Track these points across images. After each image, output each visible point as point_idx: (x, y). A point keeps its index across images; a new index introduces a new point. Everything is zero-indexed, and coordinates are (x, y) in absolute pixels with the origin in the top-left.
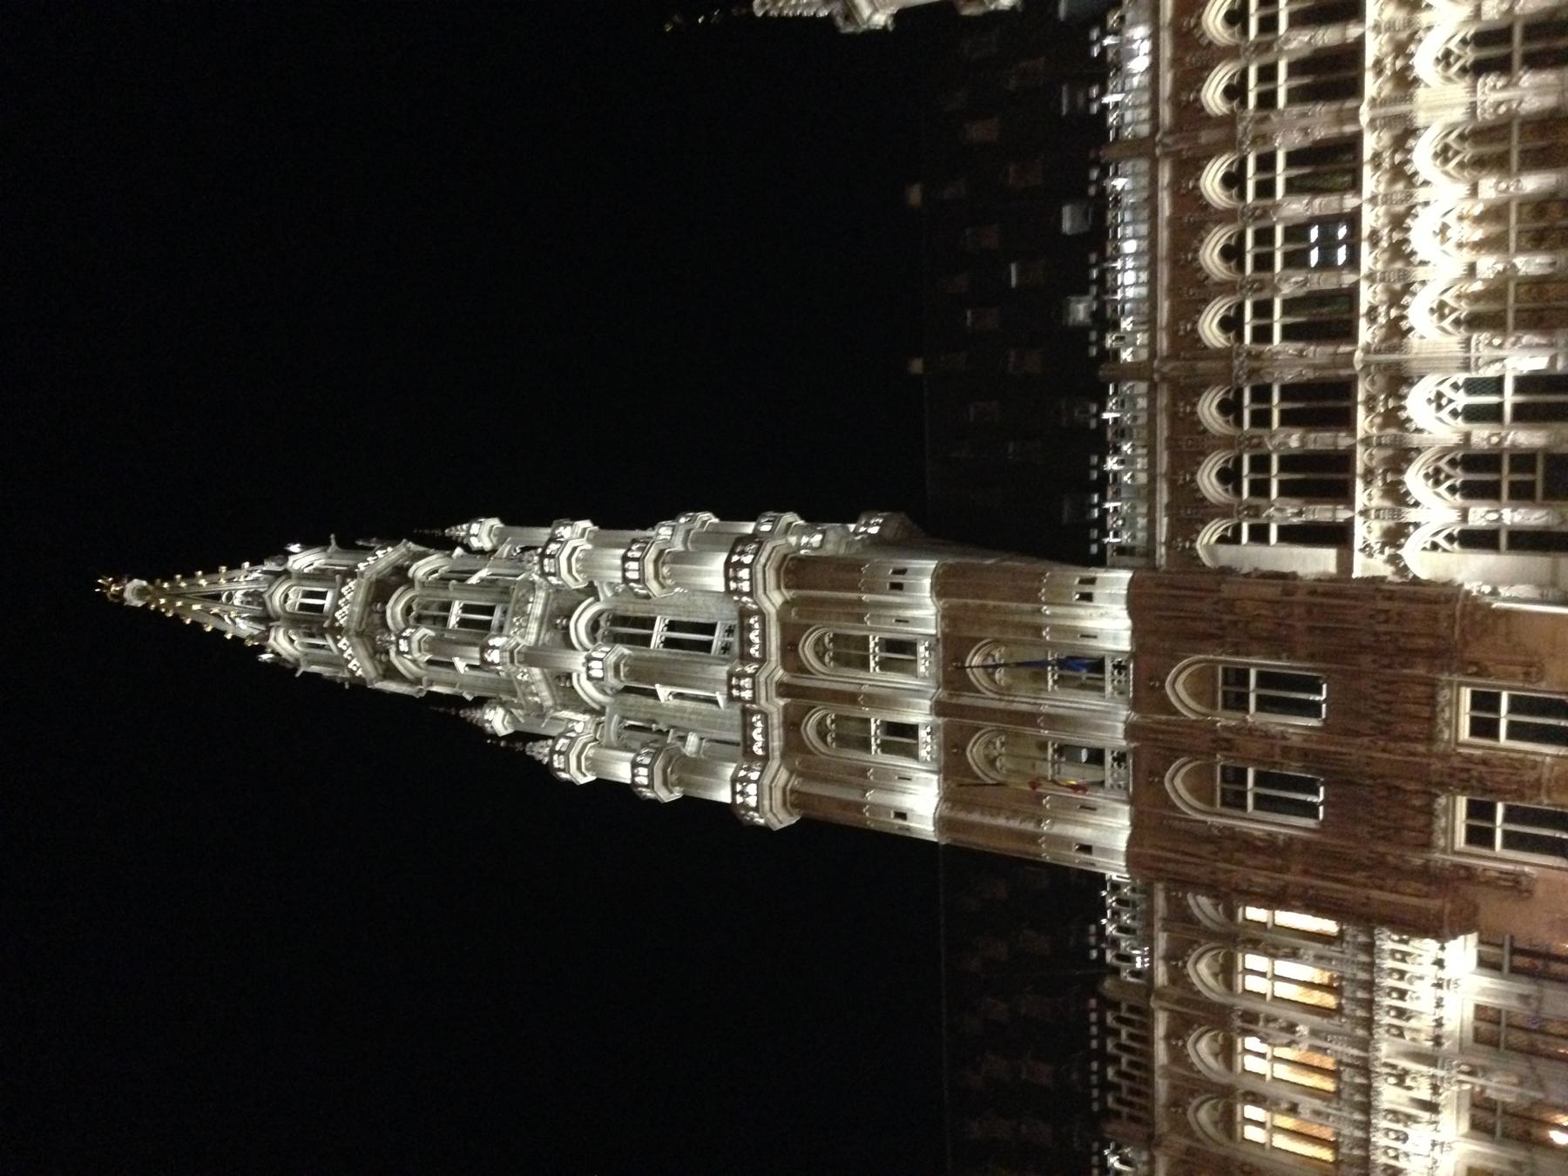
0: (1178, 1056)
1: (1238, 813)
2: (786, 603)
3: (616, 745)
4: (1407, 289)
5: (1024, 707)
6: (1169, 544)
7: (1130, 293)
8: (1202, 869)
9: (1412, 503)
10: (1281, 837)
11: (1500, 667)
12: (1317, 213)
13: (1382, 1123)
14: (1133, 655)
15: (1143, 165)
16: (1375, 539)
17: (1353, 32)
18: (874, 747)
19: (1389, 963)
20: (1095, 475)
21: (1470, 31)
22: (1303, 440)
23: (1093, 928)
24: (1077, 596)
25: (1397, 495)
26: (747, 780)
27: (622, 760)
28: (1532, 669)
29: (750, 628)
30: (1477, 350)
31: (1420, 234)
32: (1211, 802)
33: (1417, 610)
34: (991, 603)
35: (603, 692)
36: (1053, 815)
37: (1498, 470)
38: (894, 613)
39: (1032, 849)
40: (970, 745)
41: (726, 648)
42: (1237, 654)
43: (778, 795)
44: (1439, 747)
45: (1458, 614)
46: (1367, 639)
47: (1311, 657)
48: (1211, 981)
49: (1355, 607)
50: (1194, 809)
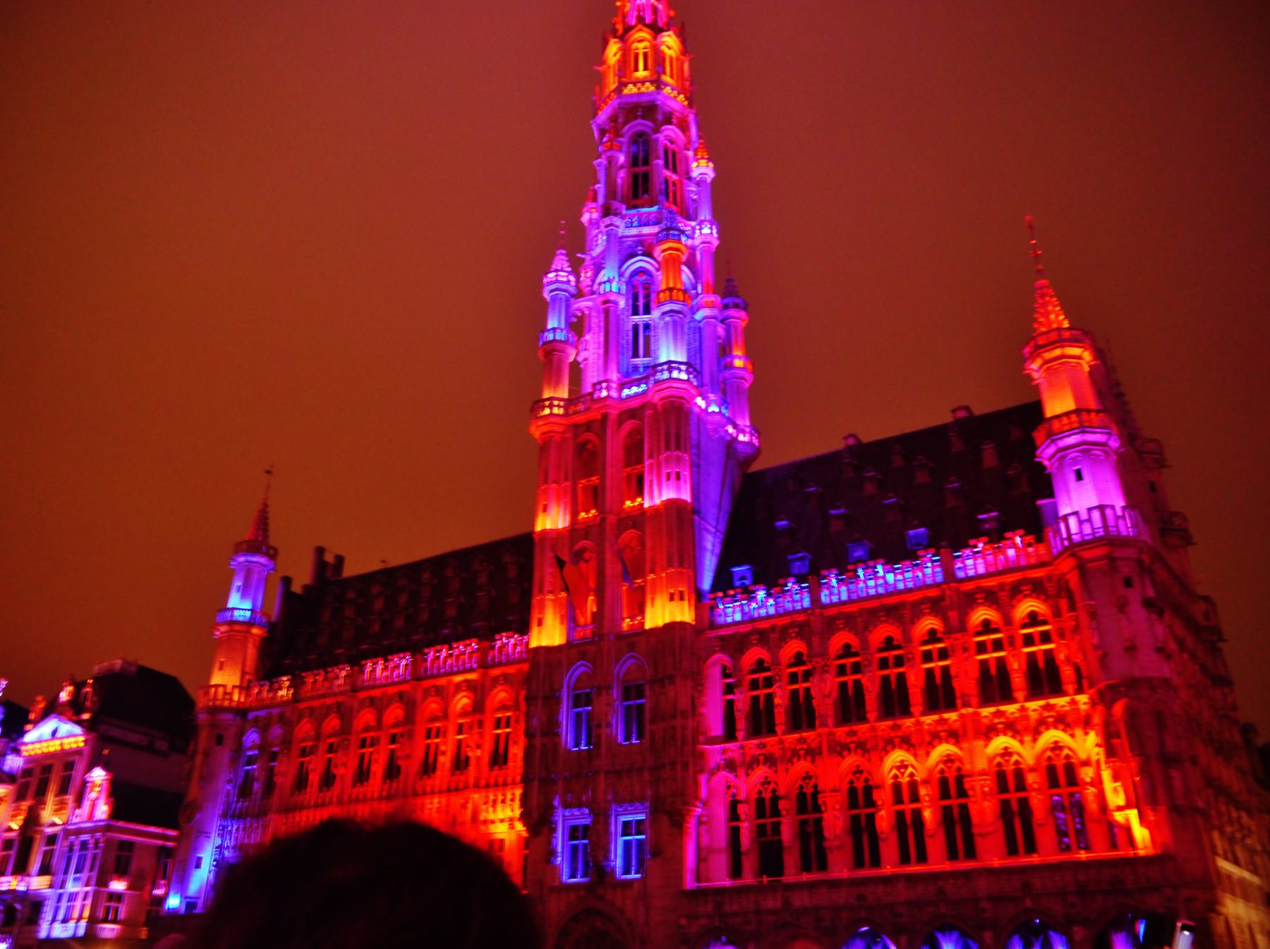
0: (458, 687)
1: (571, 705)
2: (655, 405)
3: (571, 310)
5: (609, 571)
9: (749, 772)
12: (910, 691)
13: (444, 800)
15: (939, 578)
16: (729, 755)
19: (492, 797)
26: (551, 406)
27: (559, 322)
29: (638, 386)
31: (898, 756)
38: (655, 478)
41: (636, 368)
44: (614, 807)
50: (569, 682)
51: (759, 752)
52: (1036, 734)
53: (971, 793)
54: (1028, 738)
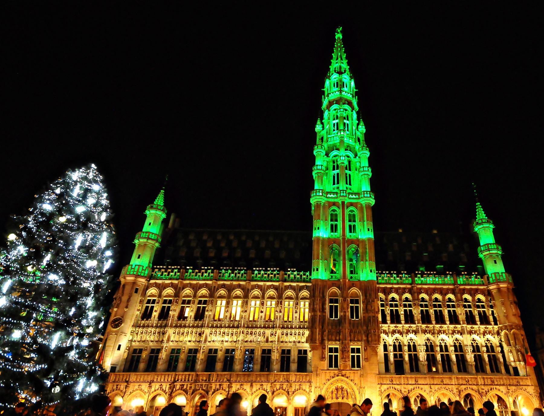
2: (361, 204)
4: (433, 334)
6: (379, 287)
10: (325, 311)
14: (359, 281)
17: (479, 323)
18: (332, 222)
20: (392, 272)
21: (479, 345)
22: (402, 314)
23: (295, 269)
25: (394, 332)
28: (366, 359)
29: (355, 195)
33: (377, 337)
34: (368, 251)
35: (333, 158)
37: (399, 351)
39: (316, 257)
42: (363, 302)
43: (320, 200)
46: (369, 328)
47: (364, 317)
51: (395, 329)
52: (484, 335)
53: (467, 351)
54: (482, 336)
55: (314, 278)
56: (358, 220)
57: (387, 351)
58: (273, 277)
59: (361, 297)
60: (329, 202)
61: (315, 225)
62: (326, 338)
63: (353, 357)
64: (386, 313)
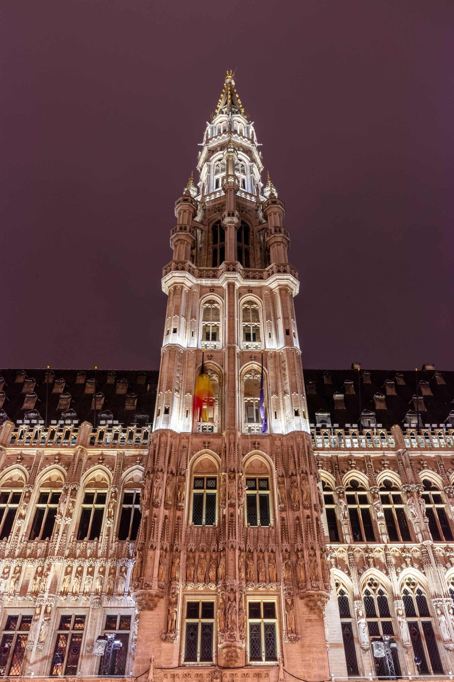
7: (435, 441)
8: (163, 465)
11: (293, 616)
22: (381, 518)
24: (296, 409)
30: (446, 601)
32: (195, 473)
34: (287, 372)
36: (182, 398)
38: (273, 332)
39: (164, 386)
40: (214, 362)
42: (279, 483)
43: (180, 280)
45: (320, 592)
47: (283, 519)
48: (91, 477)
49: (315, 540)
55: (158, 428)
56: (265, 317)
57: (349, 616)
58: (63, 437)
59: (275, 471)
60: (202, 287)
61: (170, 325)
62: (180, 574)
63: (255, 628)
64: (340, 517)
